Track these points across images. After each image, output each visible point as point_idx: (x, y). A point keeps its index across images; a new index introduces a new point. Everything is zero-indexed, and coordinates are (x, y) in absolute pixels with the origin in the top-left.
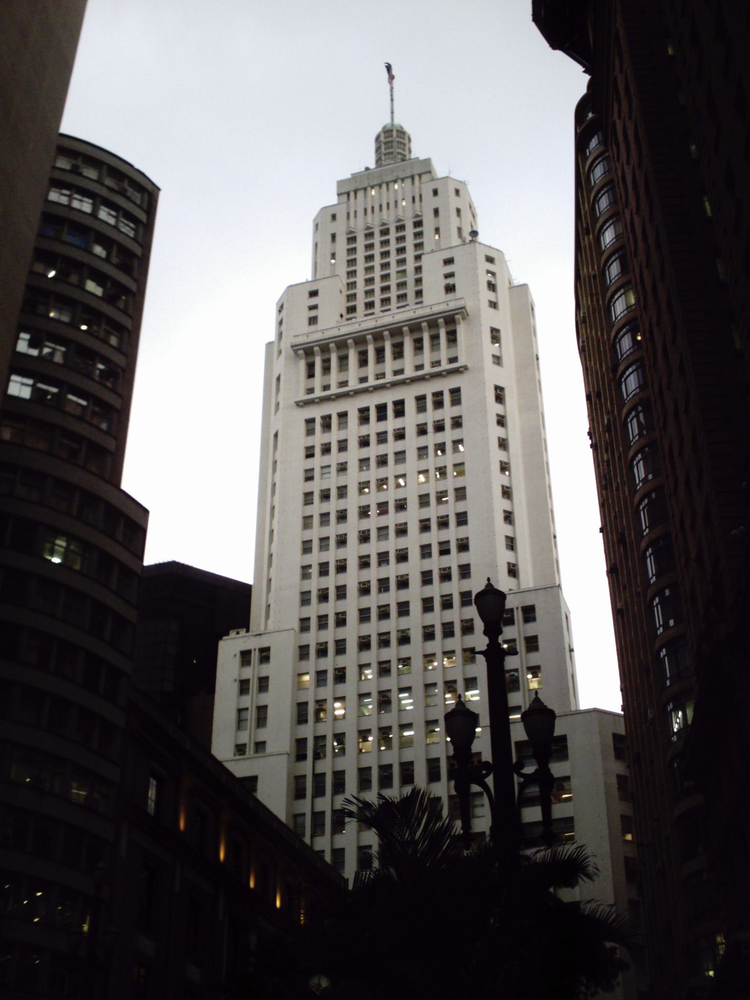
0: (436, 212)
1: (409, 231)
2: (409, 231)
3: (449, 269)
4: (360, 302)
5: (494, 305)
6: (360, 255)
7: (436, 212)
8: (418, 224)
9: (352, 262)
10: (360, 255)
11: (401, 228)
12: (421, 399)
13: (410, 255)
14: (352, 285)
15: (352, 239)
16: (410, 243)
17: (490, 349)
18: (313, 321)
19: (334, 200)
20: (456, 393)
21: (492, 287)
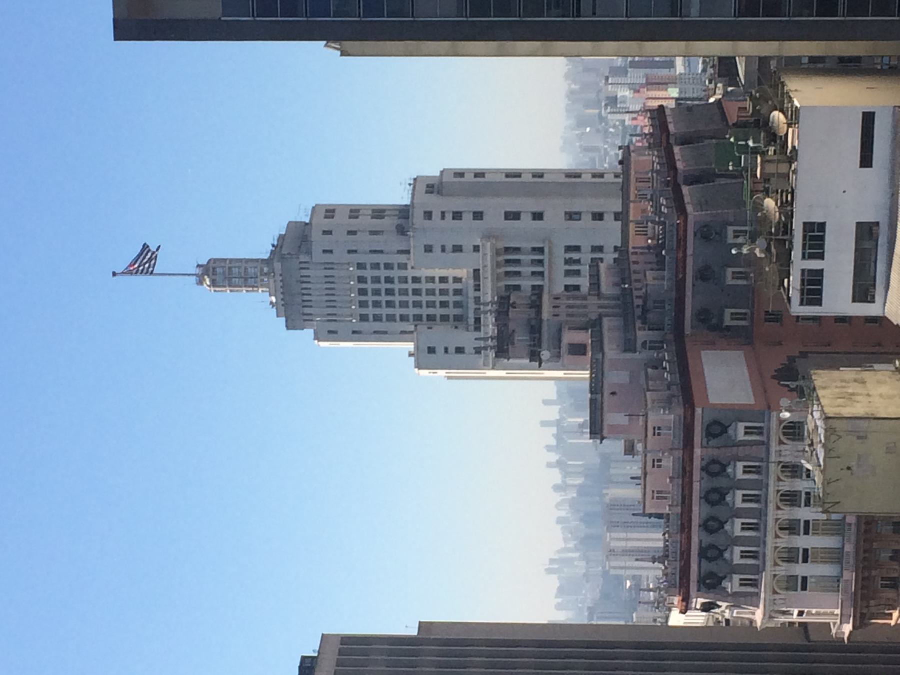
0: (350, 252)
1: (369, 274)
2: (369, 274)
3: (437, 249)
4: (439, 312)
5: (478, 216)
6: (384, 311)
7: (350, 252)
8: (361, 266)
9: (391, 318)
10: (384, 311)
11: (362, 280)
12: (568, 273)
13: (396, 274)
14: (418, 318)
15: (364, 318)
16: (383, 273)
17: (526, 221)
18: (460, 351)
19: (309, 333)
20: (569, 249)
21: (457, 216)
